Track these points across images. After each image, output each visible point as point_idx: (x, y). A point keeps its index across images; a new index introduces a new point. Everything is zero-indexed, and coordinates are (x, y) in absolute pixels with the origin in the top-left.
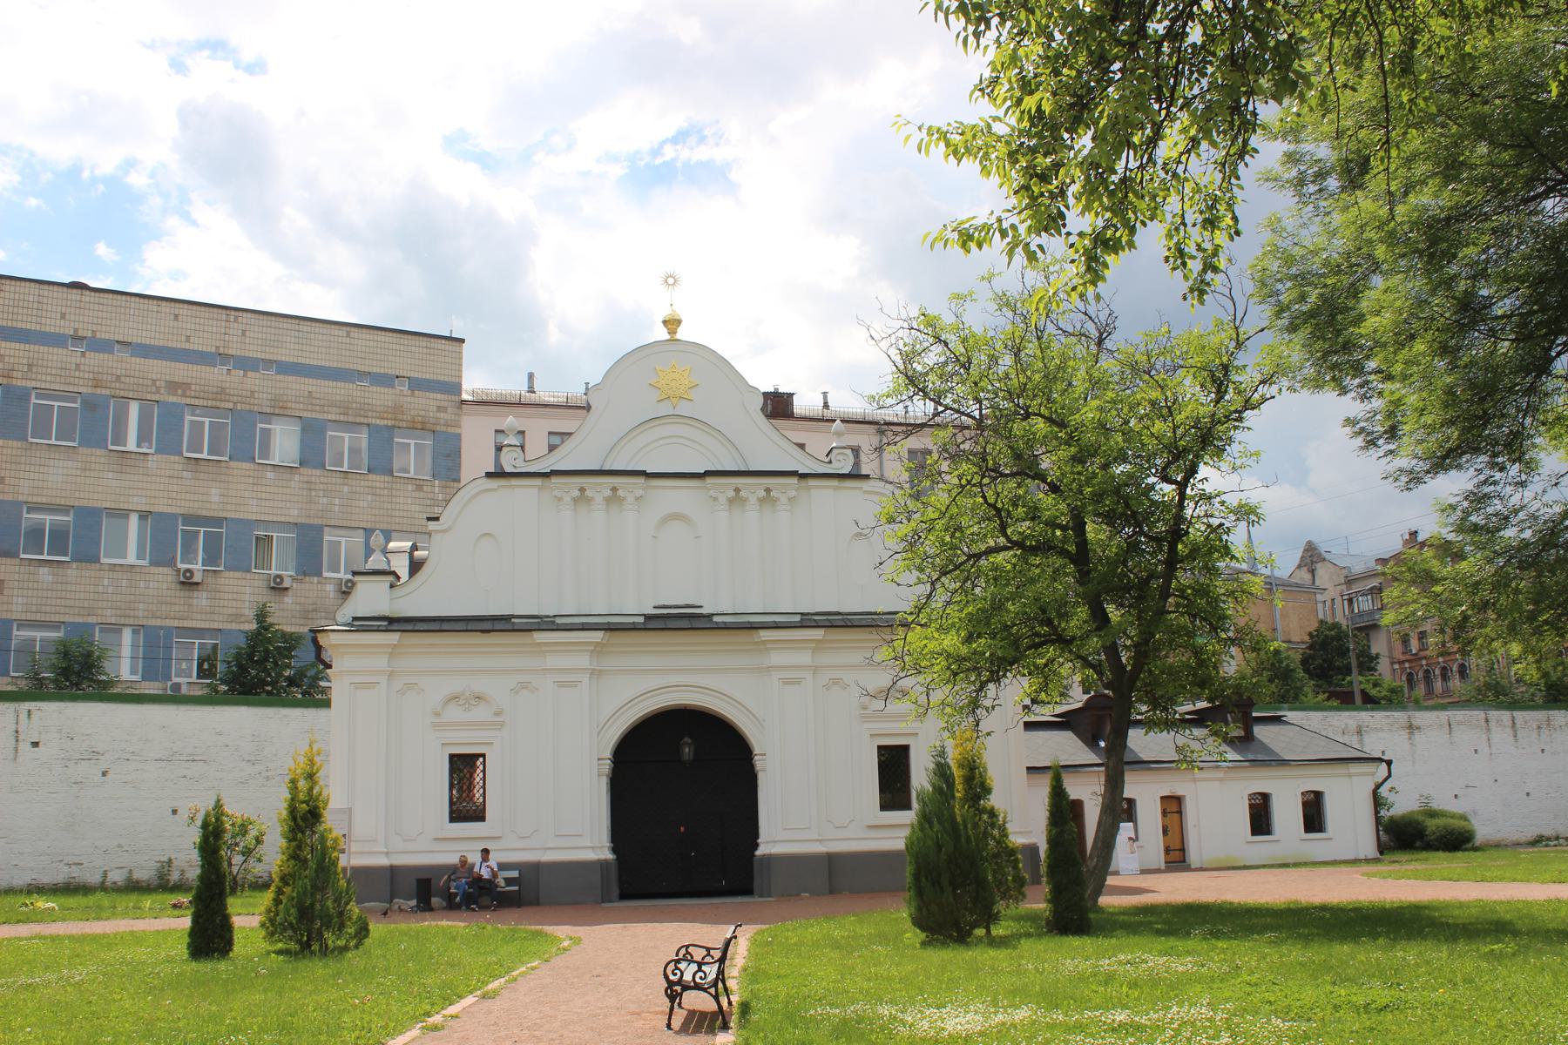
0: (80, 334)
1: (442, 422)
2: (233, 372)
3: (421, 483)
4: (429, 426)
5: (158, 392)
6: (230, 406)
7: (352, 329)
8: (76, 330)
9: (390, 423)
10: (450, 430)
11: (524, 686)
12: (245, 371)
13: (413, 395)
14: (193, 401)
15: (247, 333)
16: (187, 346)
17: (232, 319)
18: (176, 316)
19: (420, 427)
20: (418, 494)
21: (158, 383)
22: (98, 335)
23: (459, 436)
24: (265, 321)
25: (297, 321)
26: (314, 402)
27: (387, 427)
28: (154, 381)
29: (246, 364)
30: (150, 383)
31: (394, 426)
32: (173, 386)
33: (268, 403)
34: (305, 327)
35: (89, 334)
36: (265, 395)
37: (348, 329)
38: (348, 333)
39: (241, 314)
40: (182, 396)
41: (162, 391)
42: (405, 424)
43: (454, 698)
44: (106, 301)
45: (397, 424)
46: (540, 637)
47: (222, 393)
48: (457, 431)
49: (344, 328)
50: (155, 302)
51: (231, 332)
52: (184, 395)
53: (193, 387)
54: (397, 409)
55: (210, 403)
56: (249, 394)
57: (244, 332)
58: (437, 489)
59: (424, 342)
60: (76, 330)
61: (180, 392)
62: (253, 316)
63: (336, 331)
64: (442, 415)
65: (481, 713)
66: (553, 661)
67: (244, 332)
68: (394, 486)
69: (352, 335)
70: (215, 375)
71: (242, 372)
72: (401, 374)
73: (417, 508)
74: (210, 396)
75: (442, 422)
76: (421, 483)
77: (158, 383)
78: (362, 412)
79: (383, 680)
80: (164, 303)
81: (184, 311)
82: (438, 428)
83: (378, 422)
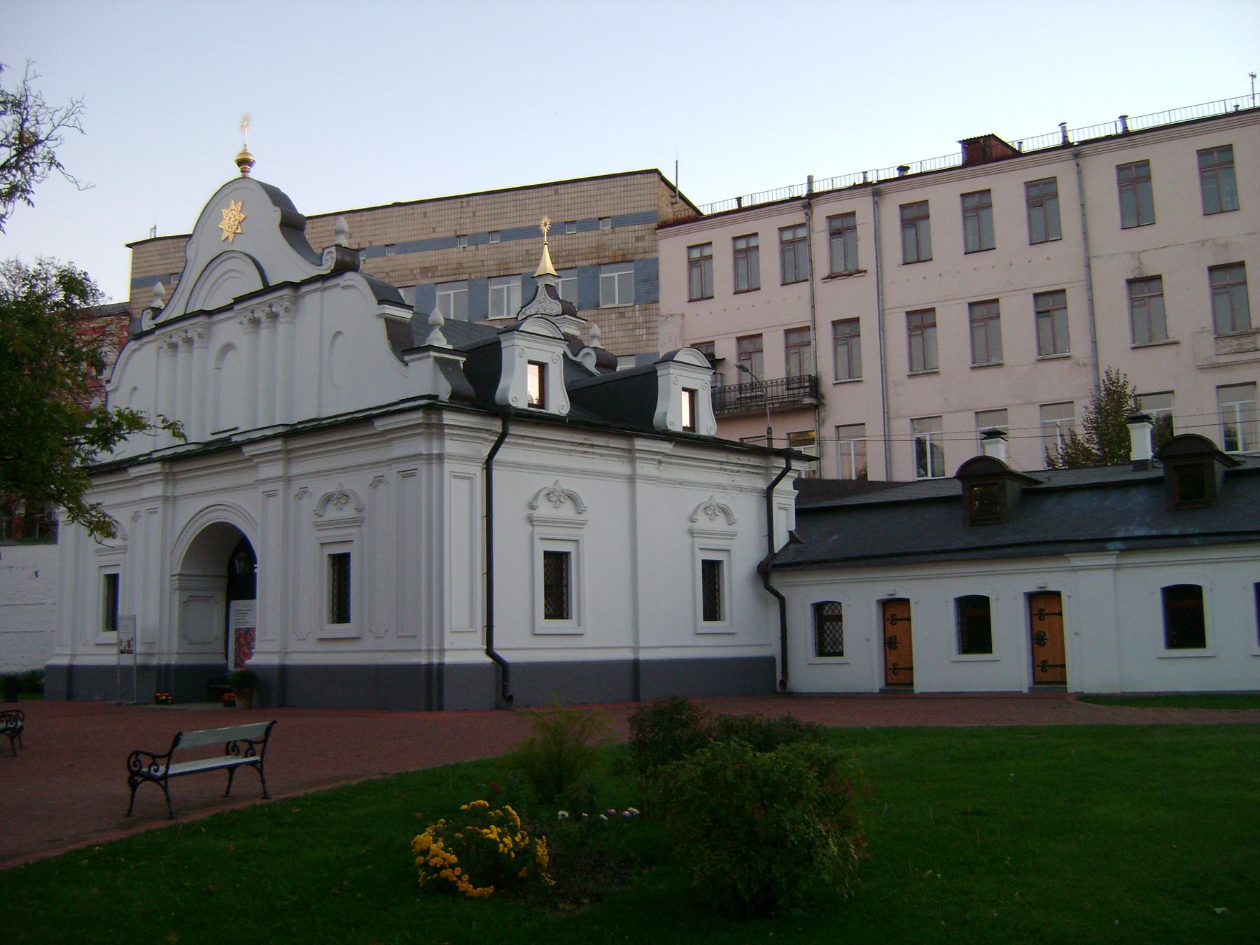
0: (362, 246)
1: (640, 250)
2: (467, 248)
3: (623, 310)
4: (629, 257)
5: (415, 278)
6: (465, 277)
7: (559, 186)
8: (359, 244)
9: (594, 262)
10: (648, 256)
11: (378, 481)
12: (476, 245)
13: (613, 232)
14: (442, 280)
15: (477, 214)
16: (436, 236)
17: (465, 204)
18: (425, 213)
19: (622, 260)
20: (621, 321)
21: (415, 272)
22: (373, 244)
23: (656, 260)
24: (489, 198)
25: (515, 192)
26: (531, 258)
27: (592, 265)
28: (412, 270)
29: (477, 239)
30: (409, 272)
31: (600, 265)
32: (425, 271)
33: (495, 267)
34: (521, 195)
35: (367, 245)
36: (492, 262)
37: (556, 187)
38: (556, 193)
39: (471, 198)
40: (431, 277)
41: (418, 277)
42: (606, 260)
43: (328, 499)
44: (377, 216)
45: (600, 261)
46: (380, 425)
47: (460, 267)
48: (654, 255)
49: (553, 187)
50: (410, 206)
51: (465, 216)
52: (433, 277)
53: (439, 268)
54: (600, 247)
55: (451, 278)
56: (480, 264)
57: (474, 215)
58: (637, 313)
59: (621, 181)
60: (359, 244)
61: (430, 274)
62: (481, 197)
63: (546, 191)
64: (640, 244)
65: (348, 512)
66: (401, 448)
67: (474, 215)
68: (600, 317)
69: (559, 191)
70: (454, 254)
71: (474, 246)
72: (602, 216)
73: (620, 334)
74: (452, 272)
75: (640, 250)
76: (623, 310)
77: (415, 272)
78: (570, 258)
79: (279, 486)
80: (416, 206)
81: (430, 208)
82: (637, 257)
83: (584, 263)
